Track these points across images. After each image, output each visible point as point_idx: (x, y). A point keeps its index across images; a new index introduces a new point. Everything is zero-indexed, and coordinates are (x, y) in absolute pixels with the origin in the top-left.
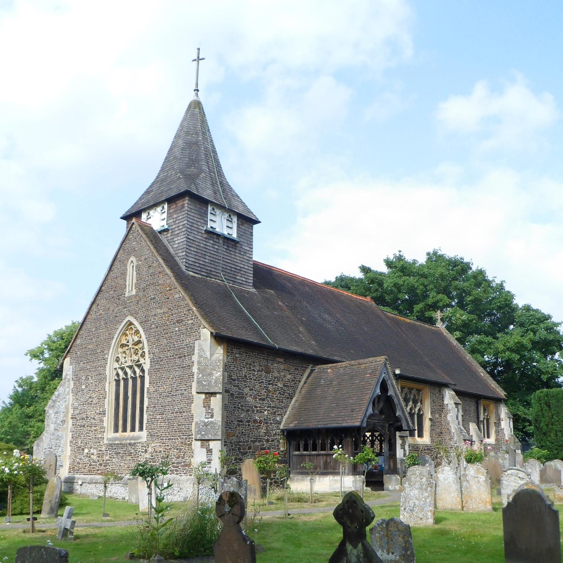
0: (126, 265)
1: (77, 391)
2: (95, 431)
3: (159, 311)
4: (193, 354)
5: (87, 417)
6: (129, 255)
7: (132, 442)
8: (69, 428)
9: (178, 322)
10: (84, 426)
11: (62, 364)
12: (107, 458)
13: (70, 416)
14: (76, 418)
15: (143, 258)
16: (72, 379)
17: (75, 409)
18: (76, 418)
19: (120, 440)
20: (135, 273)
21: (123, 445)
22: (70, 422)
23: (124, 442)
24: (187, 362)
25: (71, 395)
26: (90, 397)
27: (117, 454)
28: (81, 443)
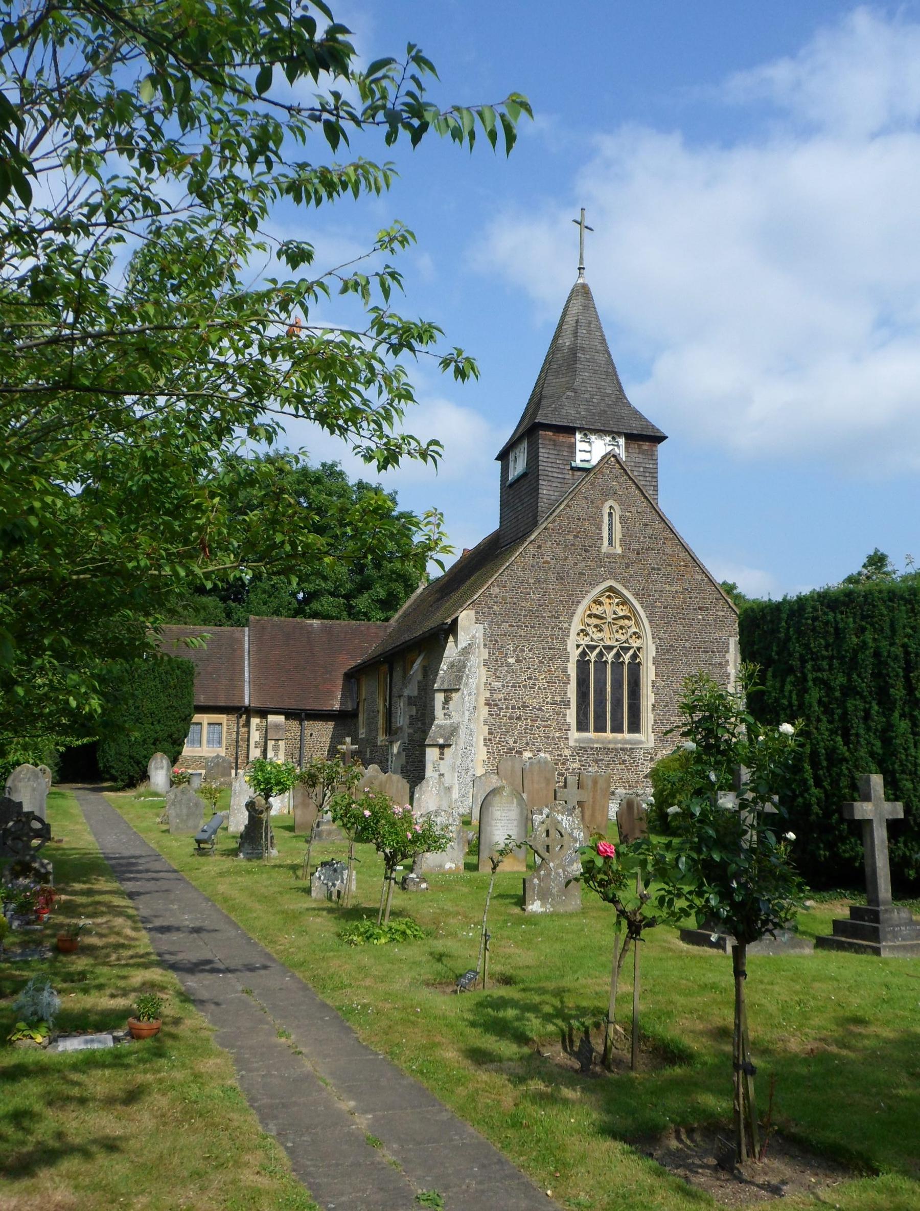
0: (599, 509)
1: (495, 664)
2: (545, 727)
3: (668, 587)
4: (727, 652)
5: (525, 706)
6: (605, 496)
7: (628, 746)
8: (482, 719)
9: (700, 608)
10: (519, 718)
11: (457, 618)
12: (576, 765)
13: (482, 701)
14: (496, 705)
15: (634, 510)
16: (485, 645)
17: (492, 691)
18: (496, 705)
19: (603, 743)
20: (617, 526)
21: (608, 751)
22: (484, 711)
23: (611, 746)
24: (717, 659)
25: (483, 670)
26: (530, 678)
27: (596, 761)
28: (515, 742)
